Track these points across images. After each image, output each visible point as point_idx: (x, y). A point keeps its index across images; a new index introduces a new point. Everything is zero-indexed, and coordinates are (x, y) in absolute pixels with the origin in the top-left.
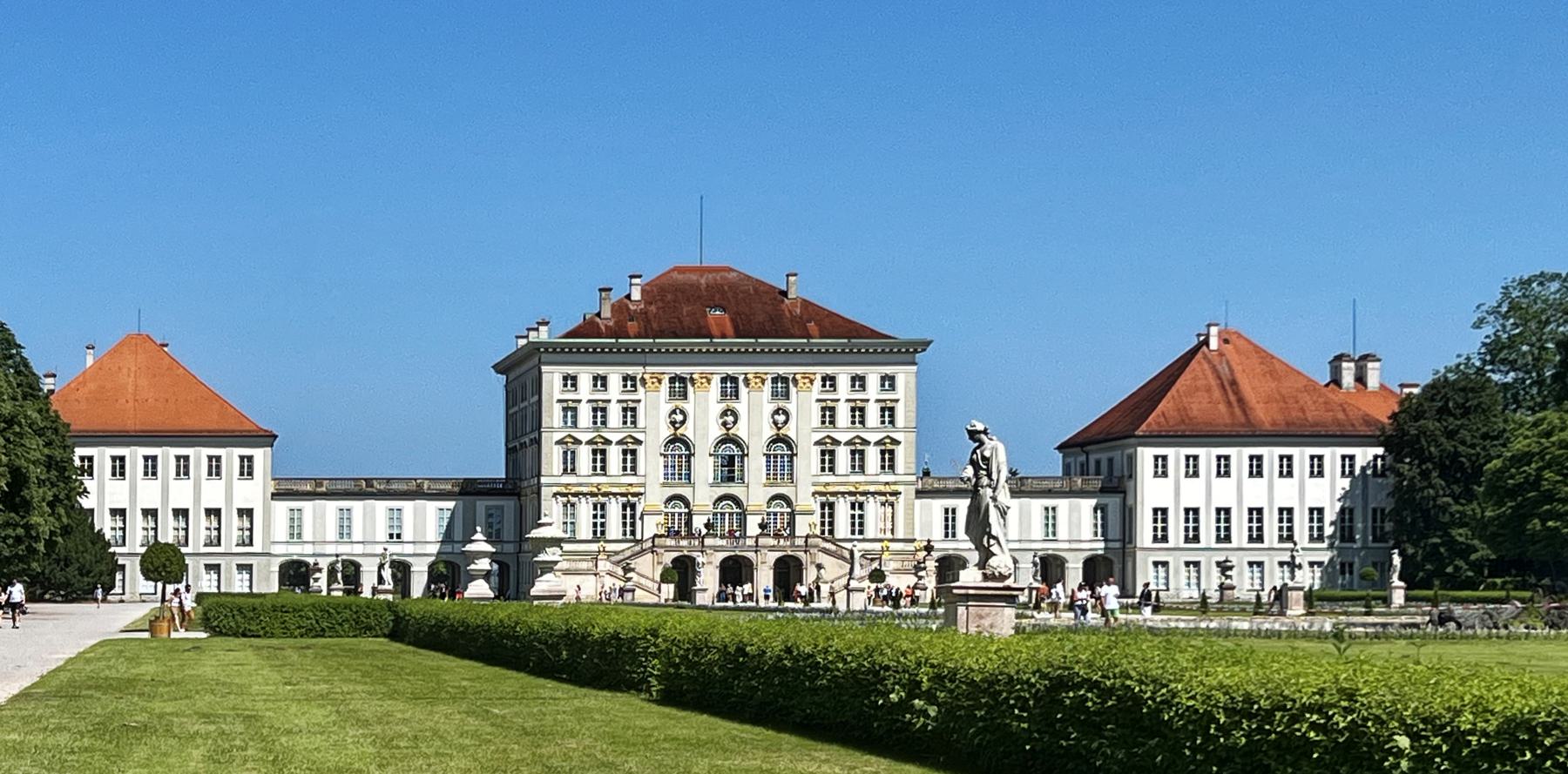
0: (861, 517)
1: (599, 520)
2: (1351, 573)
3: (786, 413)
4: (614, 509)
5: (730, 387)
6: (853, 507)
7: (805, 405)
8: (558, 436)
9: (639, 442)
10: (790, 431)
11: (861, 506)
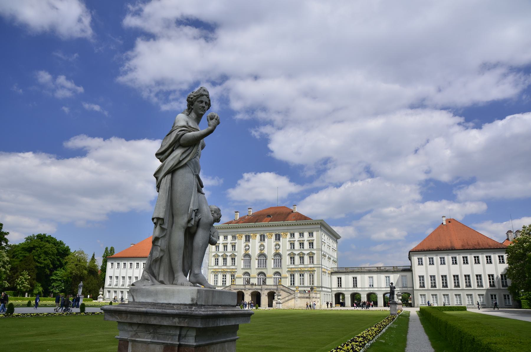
0: (303, 279)
1: (224, 280)
2: (495, 298)
3: (279, 245)
4: (228, 277)
5: (263, 238)
6: (300, 276)
7: (285, 242)
8: (213, 254)
9: (235, 256)
10: (281, 251)
11: (303, 275)
